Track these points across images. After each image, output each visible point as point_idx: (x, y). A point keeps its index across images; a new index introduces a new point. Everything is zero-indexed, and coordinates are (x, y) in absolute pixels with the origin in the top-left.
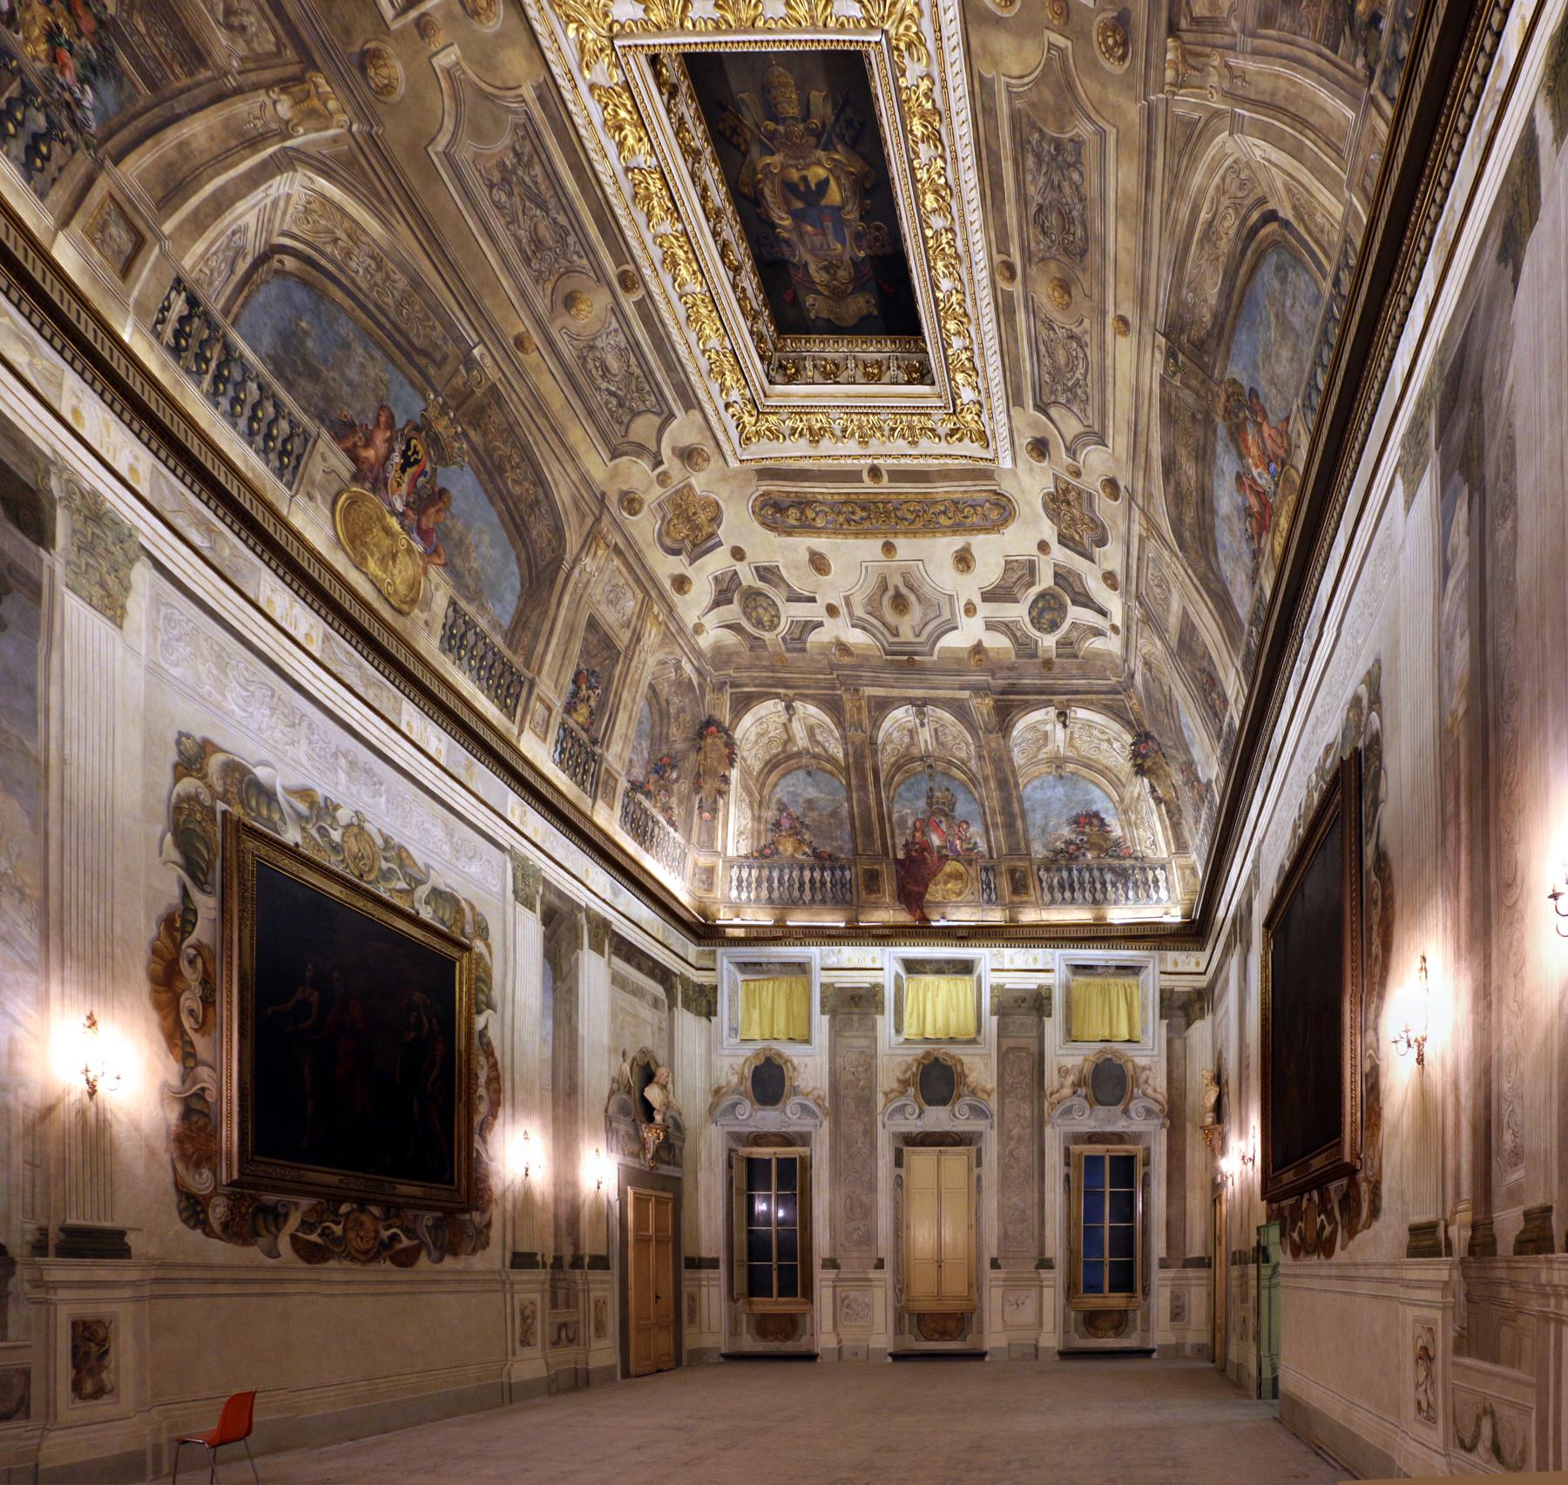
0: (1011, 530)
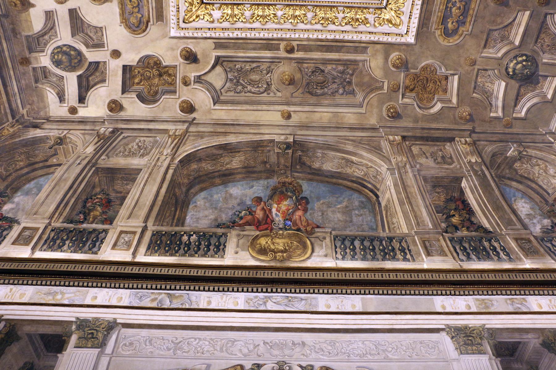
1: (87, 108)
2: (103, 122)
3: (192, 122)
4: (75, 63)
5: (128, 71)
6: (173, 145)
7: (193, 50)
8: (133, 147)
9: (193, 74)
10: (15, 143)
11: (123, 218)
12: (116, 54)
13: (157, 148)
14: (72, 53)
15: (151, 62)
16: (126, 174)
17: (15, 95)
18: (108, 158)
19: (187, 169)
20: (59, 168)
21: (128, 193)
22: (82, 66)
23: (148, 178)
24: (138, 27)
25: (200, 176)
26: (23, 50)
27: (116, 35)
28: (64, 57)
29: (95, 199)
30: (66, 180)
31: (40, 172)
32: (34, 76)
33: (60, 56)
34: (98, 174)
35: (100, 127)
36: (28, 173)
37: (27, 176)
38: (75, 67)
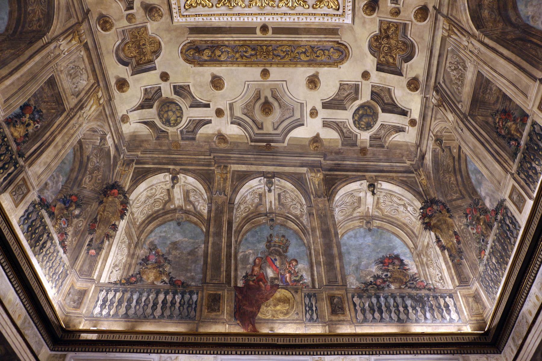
0: (345, 66)
1: (412, 111)
2: (427, 98)
3: (438, 11)
4: (371, 112)
5: (382, 67)
6: (459, 34)
7: (366, 2)
8: (455, 76)
9: (389, 4)
10: (435, 178)
11: (525, 102)
12: (366, 75)
13: (459, 51)
14: (361, 112)
15: (375, 44)
16: (480, 88)
17: (392, 166)
18: (461, 101)
19: (487, 22)
20: (463, 149)
21: (501, 90)
22: (374, 106)
23: (489, 66)
24: (342, 52)
25: (499, 8)
26: (354, 150)
27: (349, 72)
28: (364, 120)
29: (499, 125)
30: (475, 146)
31: (463, 166)
32: (377, 147)
33: (362, 123)
34: (475, 116)
35: (431, 103)
36: (462, 177)
37: (464, 178)
38: (374, 113)
